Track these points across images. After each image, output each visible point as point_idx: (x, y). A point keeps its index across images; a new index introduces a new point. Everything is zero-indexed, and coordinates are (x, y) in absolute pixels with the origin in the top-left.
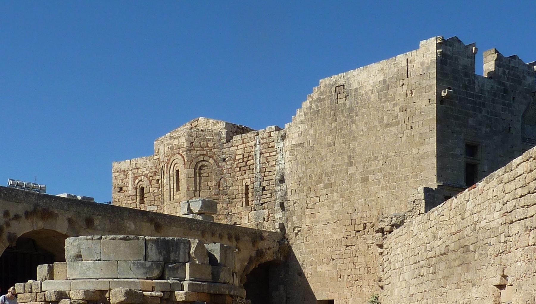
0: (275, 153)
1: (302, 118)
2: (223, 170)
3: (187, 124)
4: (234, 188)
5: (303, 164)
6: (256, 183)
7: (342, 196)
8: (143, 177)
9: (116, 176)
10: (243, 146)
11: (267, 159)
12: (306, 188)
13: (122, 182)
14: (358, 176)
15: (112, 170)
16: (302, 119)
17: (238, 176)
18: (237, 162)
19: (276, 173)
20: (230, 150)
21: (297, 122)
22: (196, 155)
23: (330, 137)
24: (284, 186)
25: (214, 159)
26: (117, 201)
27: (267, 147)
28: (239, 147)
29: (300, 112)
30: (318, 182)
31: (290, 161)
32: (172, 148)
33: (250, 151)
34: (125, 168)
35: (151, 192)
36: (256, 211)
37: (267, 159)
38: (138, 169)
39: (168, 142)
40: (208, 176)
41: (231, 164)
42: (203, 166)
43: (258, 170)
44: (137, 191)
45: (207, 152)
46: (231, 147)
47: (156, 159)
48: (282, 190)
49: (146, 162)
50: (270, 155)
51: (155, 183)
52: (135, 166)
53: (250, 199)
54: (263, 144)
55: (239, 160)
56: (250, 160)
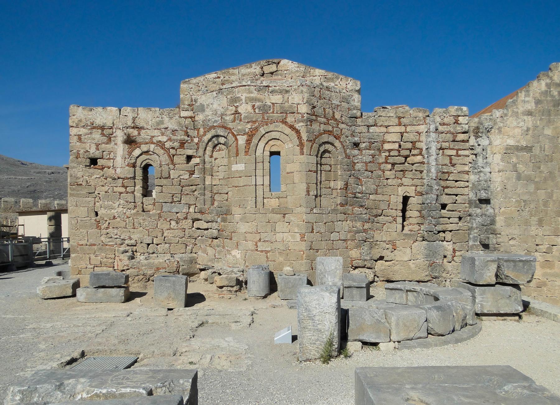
0: (467, 153)
2: (355, 164)
3: (253, 65)
4: (379, 197)
5: (529, 179)
6: (429, 196)
8: (152, 147)
9: (80, 133)
11: (451, 159)
12: (536, 219)
15: (70, 121)
16: (530, 108)
17: (387, 179)
18: (387, 154)
19: (471, 186)
20: (371, 131)
21: (519, 111)
22: (320, 130)
24: (488, 209)
25: (341, 142)
26: (84, 184)
27: (452, 139)
28: (391, 129)
29: (525, 96)
31: (503, 171)
32: (264, 109)
33: (415, 140)
34: (104, 122)
35: (172, 177)
37: (451, 159)
38: (139, 128)
39: (252, 95)
40: (330, 171)
41: (373, 156)
42: (325, 151)
44: (135, 170)
45: (333, 127)
46: (372, 126)
47: (186, 118)
48: (485, 215)
49: (160, 119)
50: (457, 153)
51: (181, 162)
52: (133, 122)
54: (442, 133)
55: (390, 151)
56: (413, 155)
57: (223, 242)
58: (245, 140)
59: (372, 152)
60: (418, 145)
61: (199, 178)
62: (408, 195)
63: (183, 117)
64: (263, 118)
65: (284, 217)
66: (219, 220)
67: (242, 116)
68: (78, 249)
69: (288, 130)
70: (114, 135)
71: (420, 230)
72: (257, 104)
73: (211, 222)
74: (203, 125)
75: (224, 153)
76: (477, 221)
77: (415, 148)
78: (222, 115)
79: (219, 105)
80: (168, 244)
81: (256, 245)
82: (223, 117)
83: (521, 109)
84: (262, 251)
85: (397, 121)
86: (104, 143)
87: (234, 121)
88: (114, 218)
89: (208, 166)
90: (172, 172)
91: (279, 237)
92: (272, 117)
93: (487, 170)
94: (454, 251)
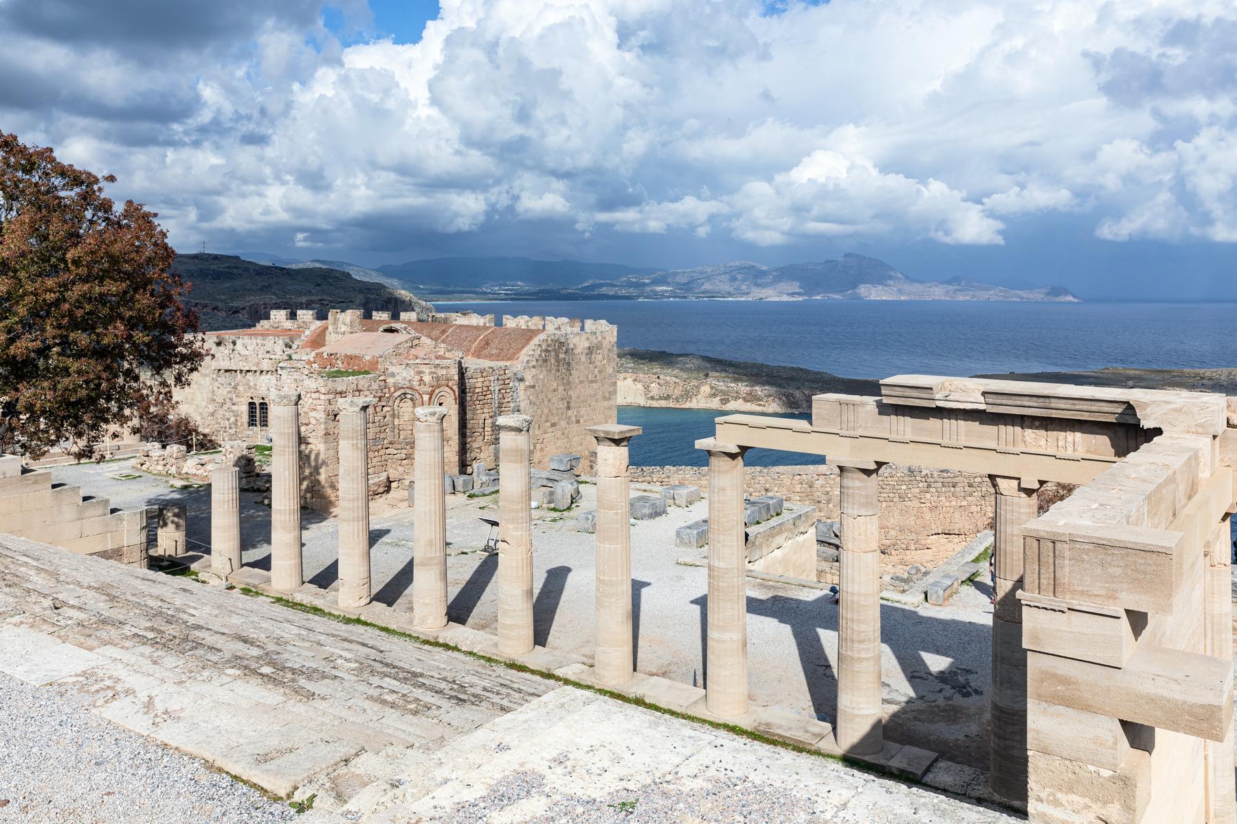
1: (534, 363)
4: (474, 422)
7: (563, 434)
10: (482, 379)
14: (574, 419)
23: (555, 384)
28: (479, 380)
30: (547, 421)
32: (438, 379)
43: (496, 405)
60: (490, 388)
66: (408, 447)
69: (449, 390)
72: (435, 375)
77: (488, 390)
78: (410, 381)
83: (530, 365)
85: (480, 374)
87: (420, 385)
89: (396, 412)
93: (518, 400)
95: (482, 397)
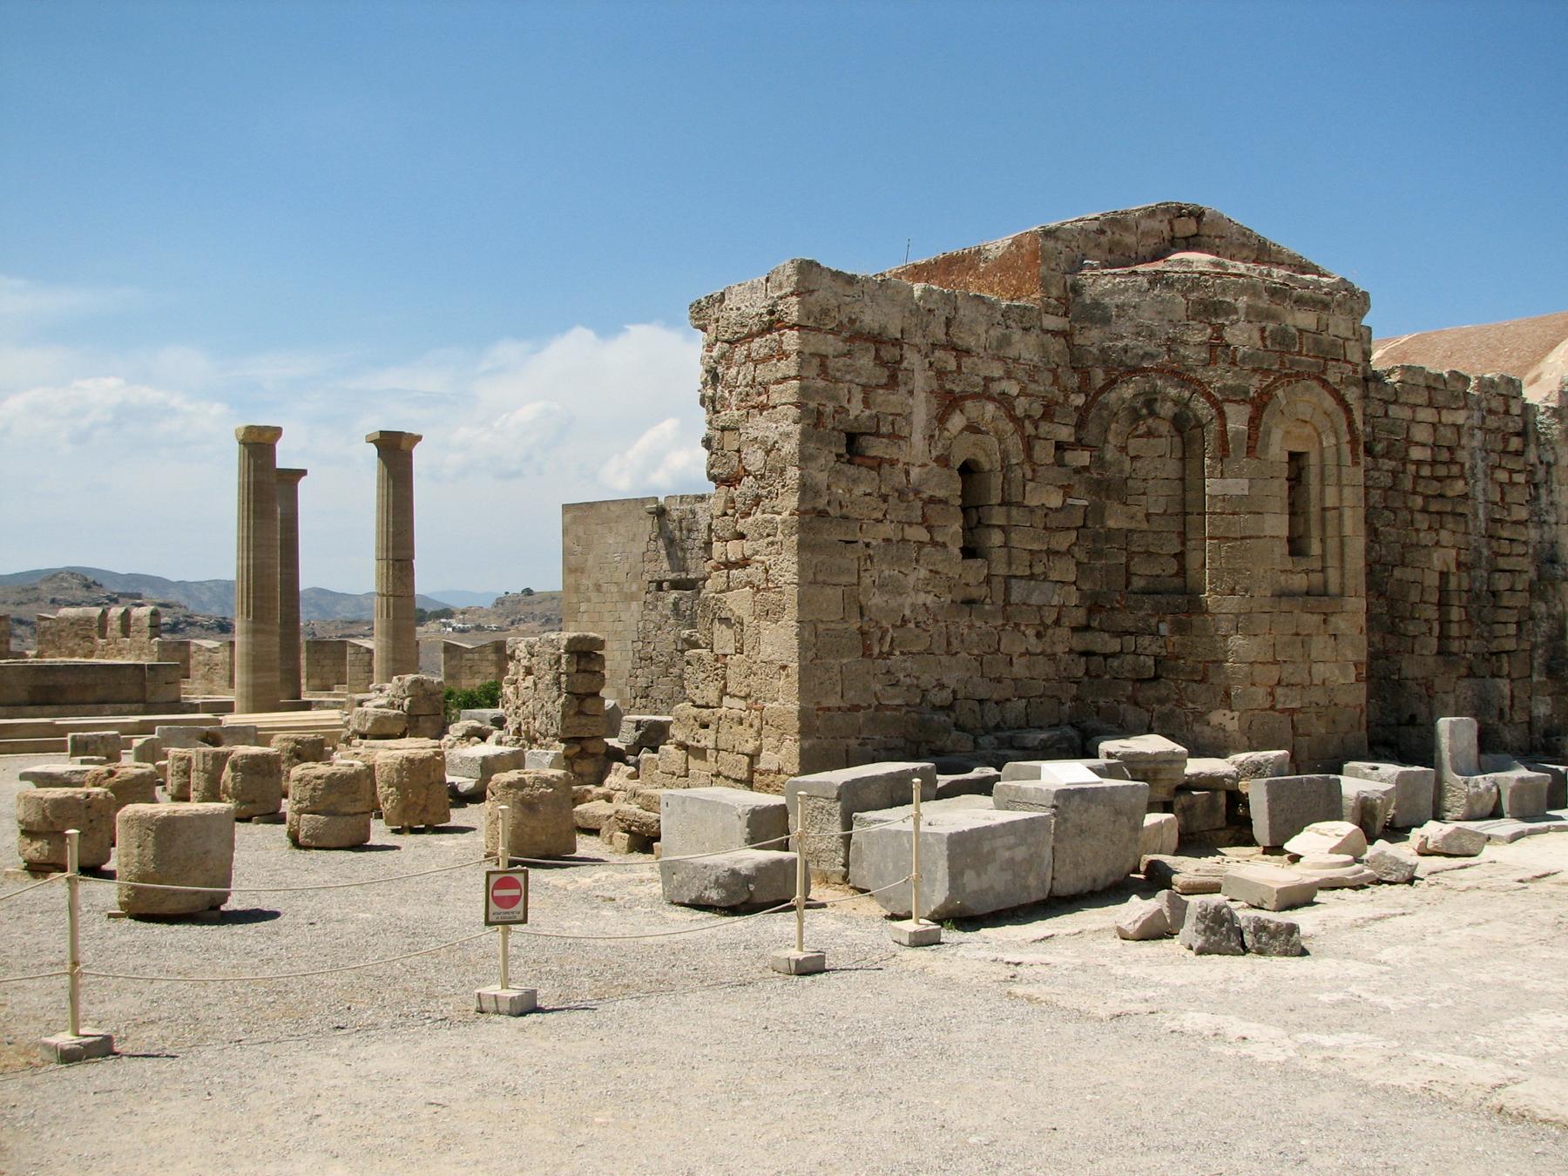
9: (823, 349)
13: (866, 403)
20: (1390, 413)
32: (1283, 340)
36: (1472, 681)
38: (962, 352)
41: (1394, 474)
47: (1055, 333)
50: (1510, 478)
53: (1454, 630)
55: (1419, 463)
57: (1177, 688)
58: (1247, 417)
59: (1394, 463)
60: (1463, 456)
61: (1087, 506)
62: (1445, 570)
63: (1048, 331)
64: (1282, 363)
65: (1325, 621)
66: (1164, 628)
67: (1239, 355)
68: (818, 723)
69: (1329, 403)
70: (905, 364)
71: (1464, 652)
72: (1271, 326)
73: (1131, 634)
74: (1105, 362)
75: (1163, 445)
76: (1542, 629)
77: (1452, 461)
79: (1160, 313)
80: (1023, 700)
81: (1272, 694)
82: (1174, 347)
84: (1282, 711)
86: (878, 386)
88: (904, 621)
90: (1030, 486)
91: (1320, 670)
92: (1299, 363)
94: (1512, 697)
95: (1433, 489)
